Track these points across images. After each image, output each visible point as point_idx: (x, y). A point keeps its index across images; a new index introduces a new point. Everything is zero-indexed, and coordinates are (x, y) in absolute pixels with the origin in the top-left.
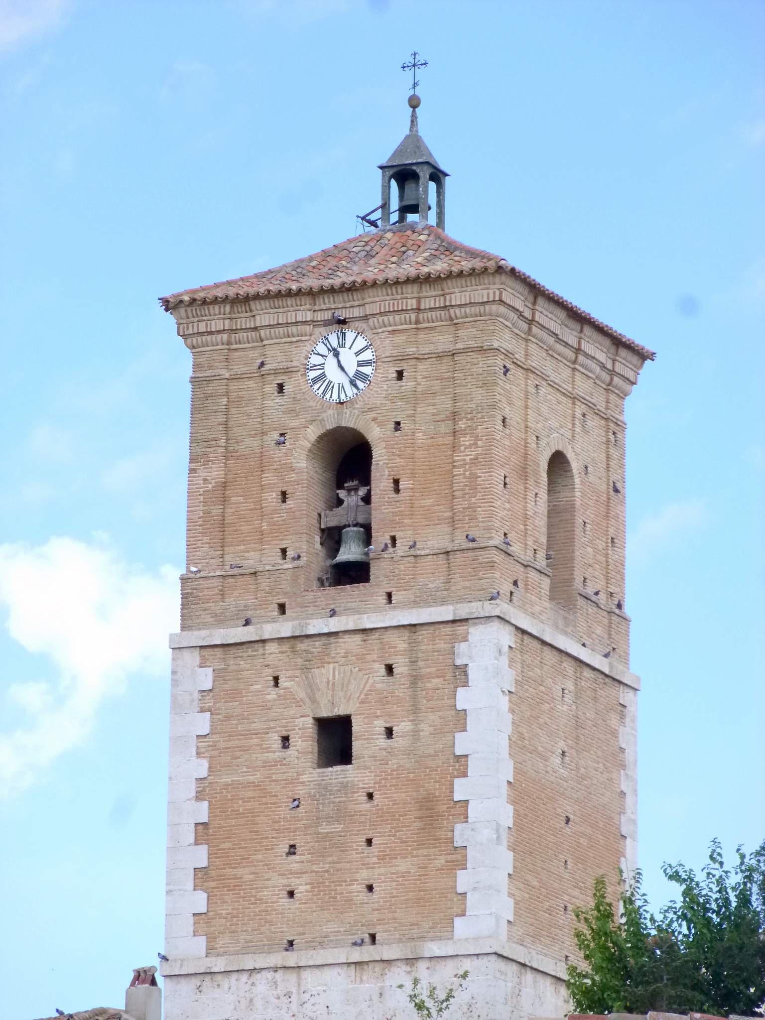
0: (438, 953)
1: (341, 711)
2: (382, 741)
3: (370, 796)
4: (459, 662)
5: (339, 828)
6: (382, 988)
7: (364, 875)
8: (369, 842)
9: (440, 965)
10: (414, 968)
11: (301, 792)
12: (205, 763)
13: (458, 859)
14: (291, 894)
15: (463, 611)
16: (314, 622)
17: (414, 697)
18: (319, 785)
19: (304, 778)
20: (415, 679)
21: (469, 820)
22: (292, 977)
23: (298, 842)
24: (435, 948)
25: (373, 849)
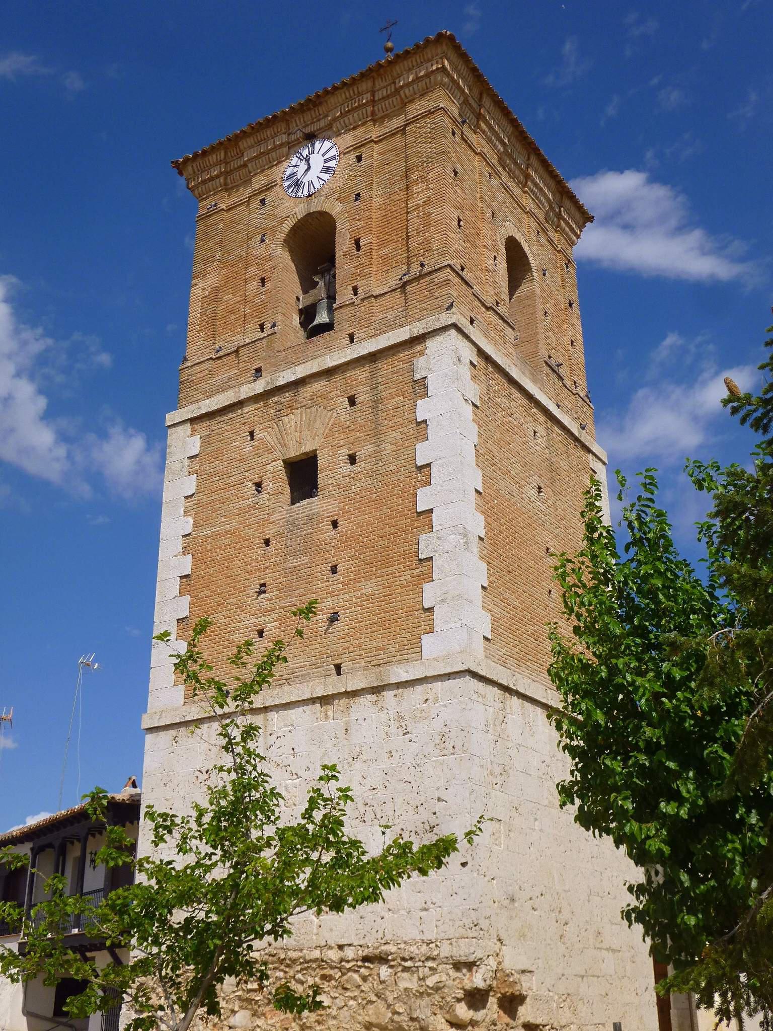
0: (405, 677)
1: (307, 448)
2: (347, 469)
3: (335, 524)
4: (417, 377)
5: (305, 559)
6: (347, 723)
8: (334, 570)
11: (270, 532)
12: (190, 520)
15: (419, 328)
17: (377, 423)
19: (275, 517)
20: (376, 404)
23: (268, 581)
24: (401, 673)
25: (337, 576)
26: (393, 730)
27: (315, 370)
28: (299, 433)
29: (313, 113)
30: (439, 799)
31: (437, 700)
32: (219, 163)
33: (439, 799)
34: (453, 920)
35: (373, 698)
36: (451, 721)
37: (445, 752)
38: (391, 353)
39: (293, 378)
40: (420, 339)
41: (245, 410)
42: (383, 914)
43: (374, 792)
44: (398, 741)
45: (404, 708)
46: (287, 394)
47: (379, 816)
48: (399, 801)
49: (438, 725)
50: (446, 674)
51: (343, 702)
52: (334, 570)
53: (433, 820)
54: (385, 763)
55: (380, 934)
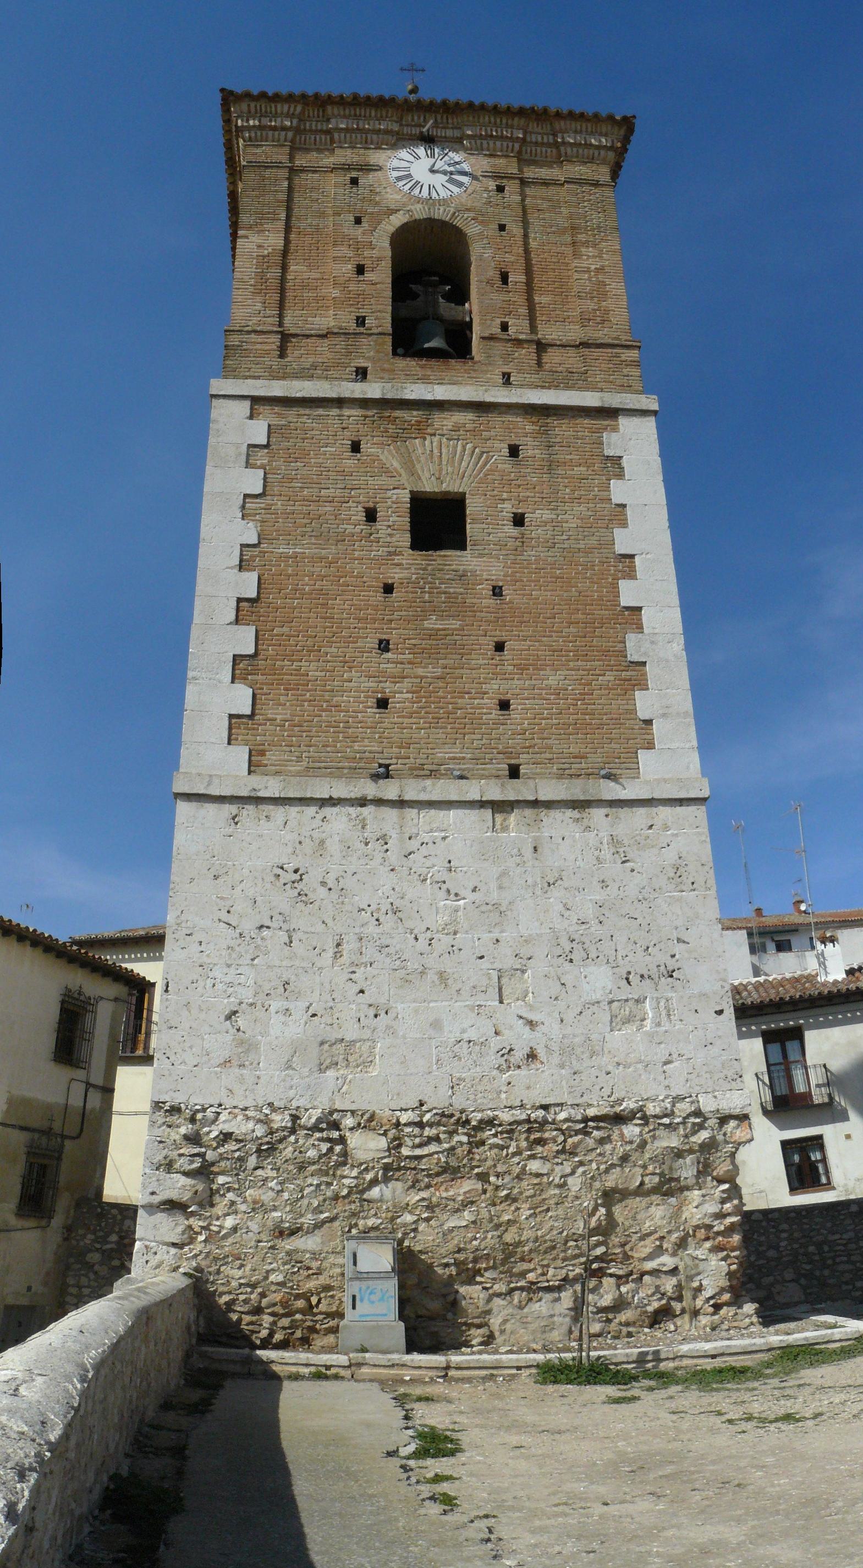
1: (451, 485)
3: (497, 591)
5: (456, 624)
6: (536, 839)
7: (496, 688)
8: (500, 647)
9: (624, 812)
10: (585, 815)
13: (634, 675)
14: (383, 704)
16: (414, 387)
18: (425, 569)
21: (646, 631)
22: (391, 814)
26: (606, 853)
27: (464, 397)
28: (442, 463)
29: (439, 117)
30: (679, 940)
31: (666, 828)
32: (290, 116)
33: (679, 940)
34: (710, 1072)
35: (575, 814)
36: (688, 853)
37: (684, 888)
38: (570, 414)
39: (429, 397)
40: (610, 413)
41: (347, 412)
42: (610, 1068)
43: (584, 927)
44: (613, 869)
45: (621, 830)
46: (415, 413)
47: (593, 955)
48: (621, 939)
49: (670, 856)
50: (676, 800)
51: (528, 812)
52: (500, 647)
53: (672, 964)
54: (599, 896)
55: (606, 1092)
